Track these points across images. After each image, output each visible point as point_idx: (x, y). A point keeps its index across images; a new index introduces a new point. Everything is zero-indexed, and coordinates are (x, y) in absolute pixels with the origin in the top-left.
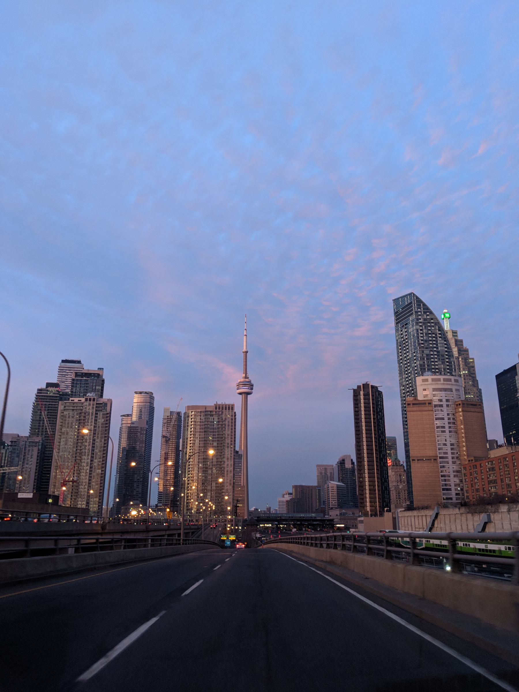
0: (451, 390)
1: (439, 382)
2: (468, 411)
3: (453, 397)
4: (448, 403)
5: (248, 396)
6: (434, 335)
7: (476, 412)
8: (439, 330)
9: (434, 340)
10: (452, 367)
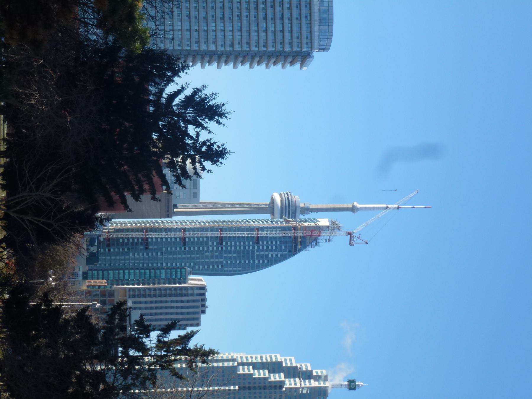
3: (177, 188)
6: (274, 247)
8: (281, 255)
9: (267, 247)
10: (234, 268)
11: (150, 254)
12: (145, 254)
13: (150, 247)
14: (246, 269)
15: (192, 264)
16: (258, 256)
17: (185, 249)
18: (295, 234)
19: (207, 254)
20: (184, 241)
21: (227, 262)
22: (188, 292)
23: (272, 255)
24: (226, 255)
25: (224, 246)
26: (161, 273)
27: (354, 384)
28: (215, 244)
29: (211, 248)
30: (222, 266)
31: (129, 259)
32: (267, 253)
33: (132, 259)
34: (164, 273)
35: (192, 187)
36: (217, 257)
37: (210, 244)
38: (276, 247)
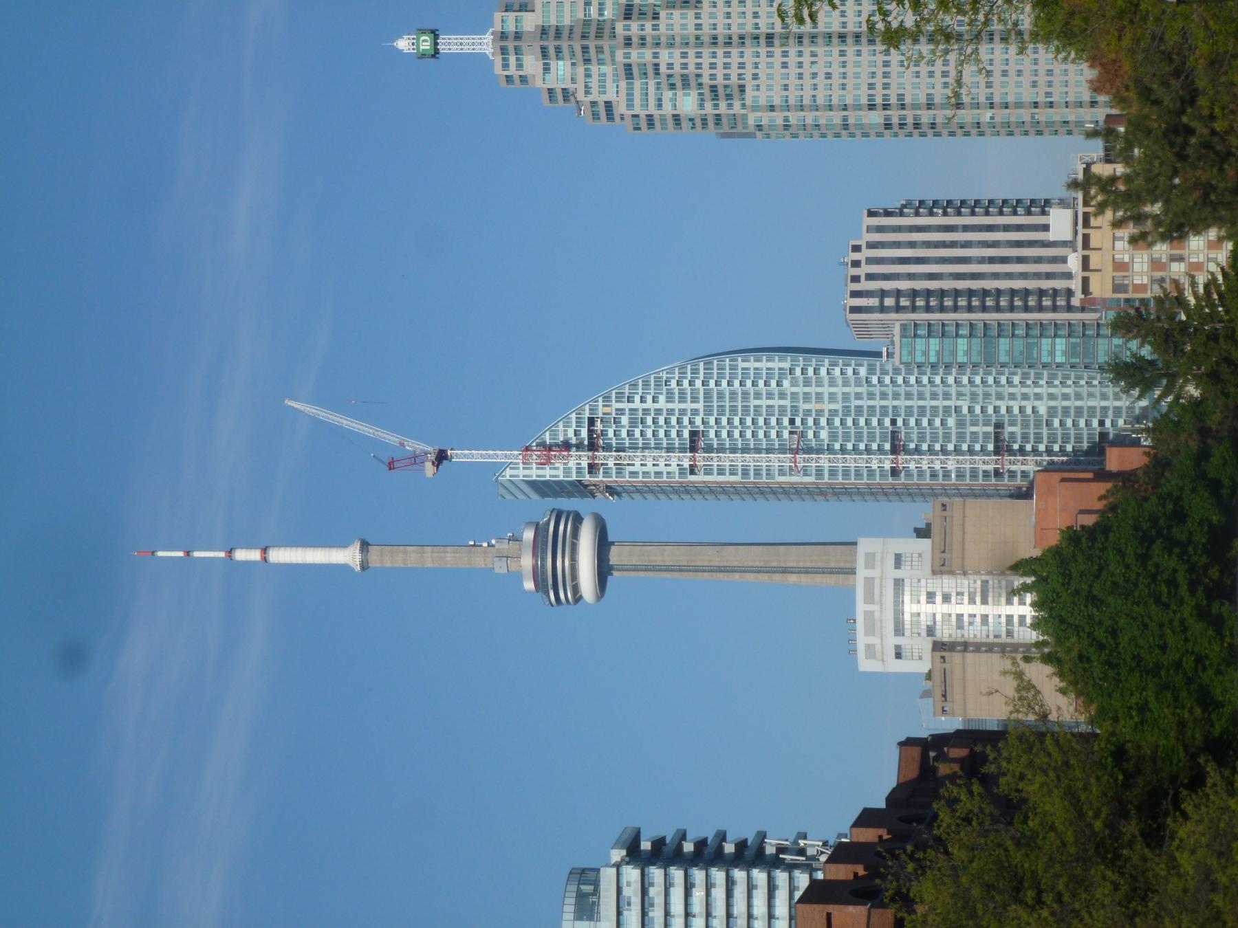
0: (899, 584)
1: (877, 615)
2: (963, 549)
4: (939, 599)
5: (610, 539)
6: (649, 420)
7: (963, 525)
8: (630, 400)
11: (990, 410)
12: (1003, 411)
13: (990, 429)
14: (727, 365)
15: (875, 380)
16: (695, 399)
17: (894, 422)
18: (593, 455)
19: (833, 406)
20: (897, 443)
21: (779, 384)
22: (897, 302)
23: (655, 400)
24: (782, 402)
25: (785, 428)
26: (968, 353)
27: (422, 47)
28: (810, 434)
29: (823, 421)
30: (791, 371)
31: (1052, 397)
32: (670, 406)
33: (1038, 397)
34: (960, 353)
35: (877, 582)
36: (807, 397)
37: (824, 434)
38: (643, 421)
